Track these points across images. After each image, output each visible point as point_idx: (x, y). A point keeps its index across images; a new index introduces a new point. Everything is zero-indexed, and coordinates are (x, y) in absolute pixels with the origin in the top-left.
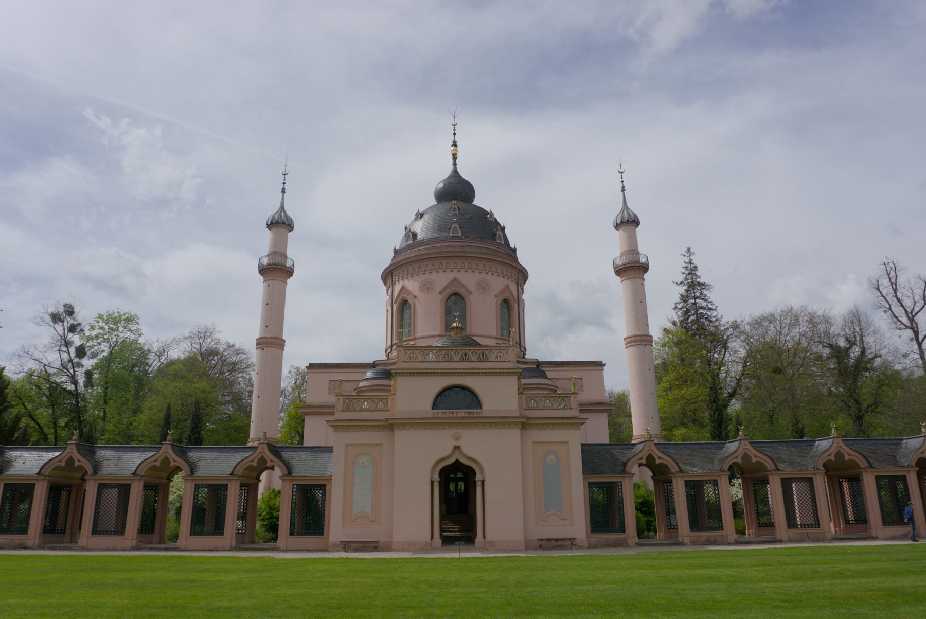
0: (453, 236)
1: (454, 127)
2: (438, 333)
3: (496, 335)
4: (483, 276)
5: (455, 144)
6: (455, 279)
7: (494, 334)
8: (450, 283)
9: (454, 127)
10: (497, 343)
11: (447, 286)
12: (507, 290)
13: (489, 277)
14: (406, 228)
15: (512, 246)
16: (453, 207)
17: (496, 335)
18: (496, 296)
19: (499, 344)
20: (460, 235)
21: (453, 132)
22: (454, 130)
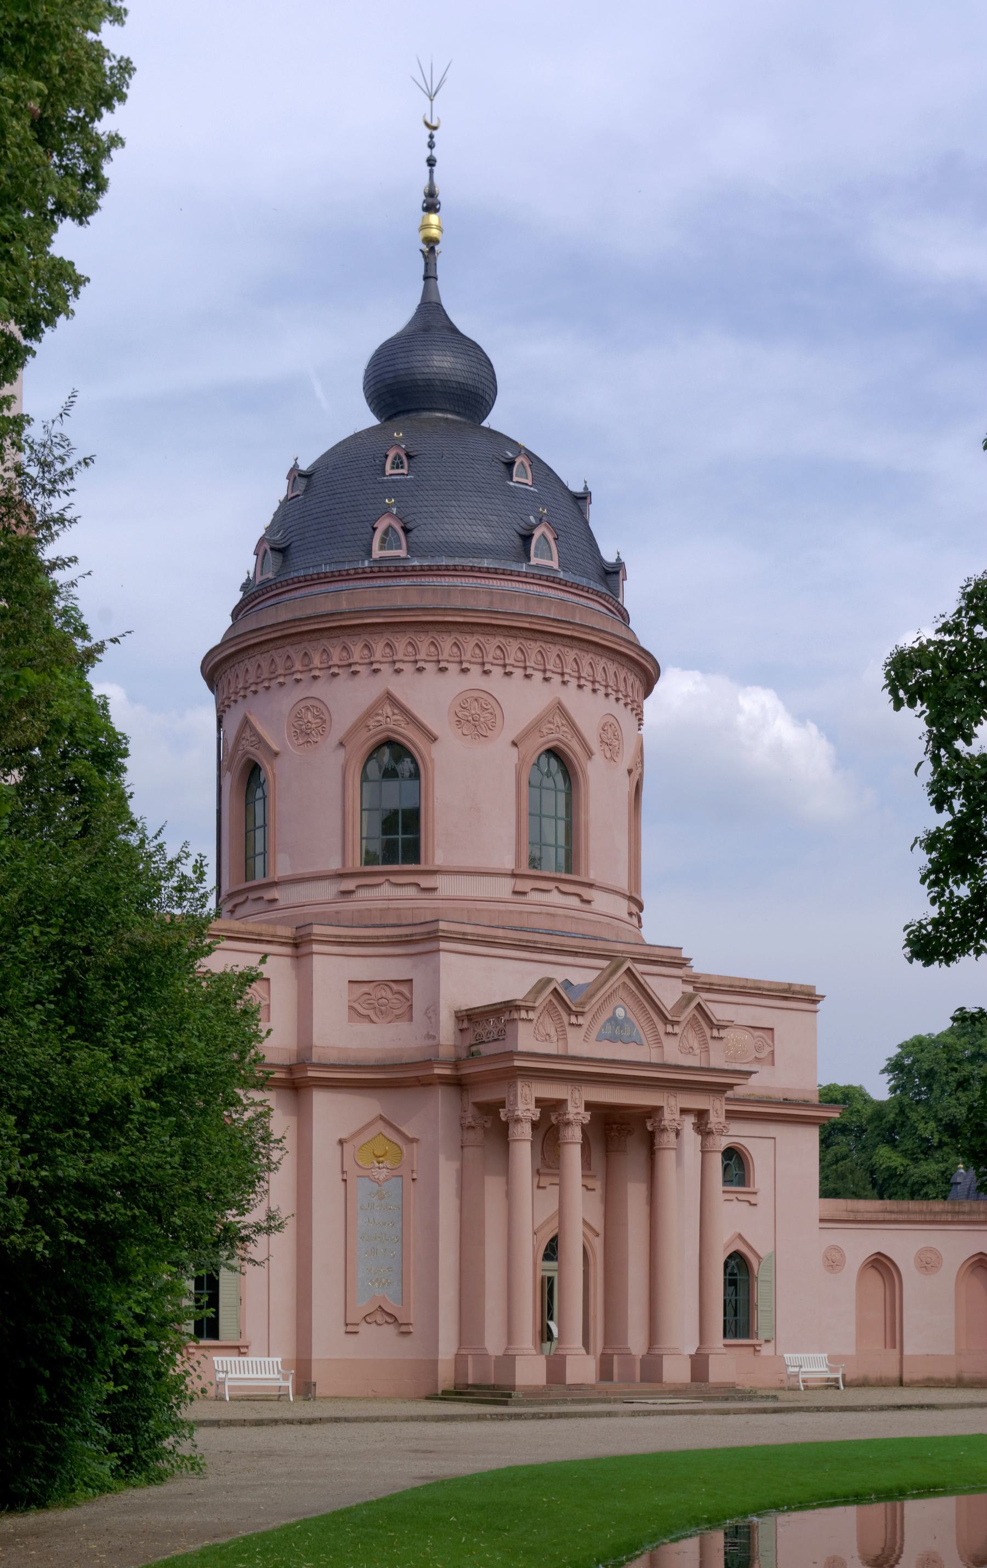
0: (383, 559)
1: (431, 137)
2: (335, 864)
3: (513, 867)
4: (475, 679)
6: (390, 698)
7: (508, 864)
8: (371, 712)
9: (431, 137)
10: (515, 893)
11: (361, 723)
12: (558, 720)
13: (496, 684)
16: (392, 454)
17: (513, 867)
19: (524, 893)
21: (427, 153)
22: (431, 146)
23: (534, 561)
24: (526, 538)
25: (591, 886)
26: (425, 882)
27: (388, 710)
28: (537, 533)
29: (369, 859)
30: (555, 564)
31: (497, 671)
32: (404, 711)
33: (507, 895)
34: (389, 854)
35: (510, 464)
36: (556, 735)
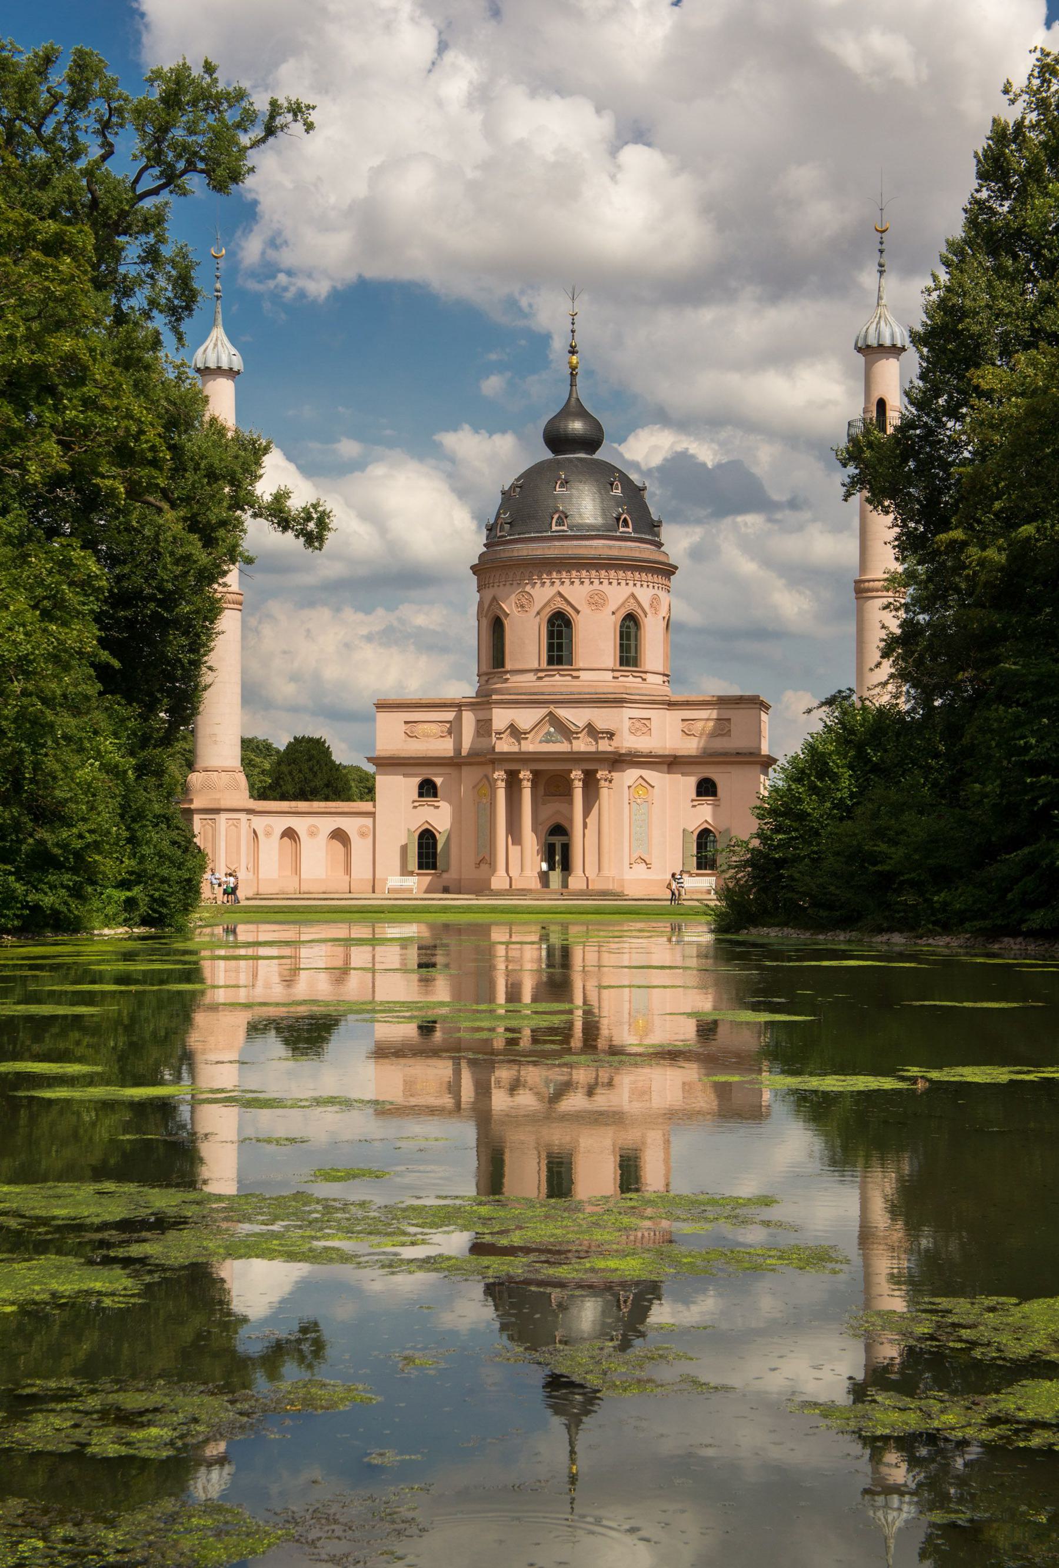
2: (535, 666)
5: (573, 351)
6: (560, 594)
7: (611, 665)
12: (632, 601)
14: (503, 493)
15: (655, 517)
18: (613, 613)
20: (565, 528)
23: (621, 529)
24: (618, 519)
25: (646, 672)
26: (575, 674)
27: (559, 599)
28: (623, 517)
29: (550, 661)
30: (630, 530)
31: (606, 582)
32: (566, 600)
33: (611, 678)
34: (560, 661)
35: (612, 484)
36: (632, 606)
